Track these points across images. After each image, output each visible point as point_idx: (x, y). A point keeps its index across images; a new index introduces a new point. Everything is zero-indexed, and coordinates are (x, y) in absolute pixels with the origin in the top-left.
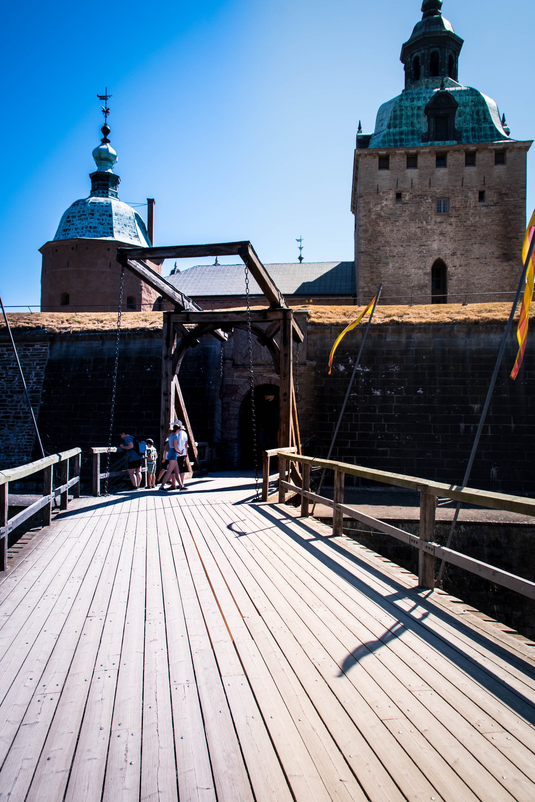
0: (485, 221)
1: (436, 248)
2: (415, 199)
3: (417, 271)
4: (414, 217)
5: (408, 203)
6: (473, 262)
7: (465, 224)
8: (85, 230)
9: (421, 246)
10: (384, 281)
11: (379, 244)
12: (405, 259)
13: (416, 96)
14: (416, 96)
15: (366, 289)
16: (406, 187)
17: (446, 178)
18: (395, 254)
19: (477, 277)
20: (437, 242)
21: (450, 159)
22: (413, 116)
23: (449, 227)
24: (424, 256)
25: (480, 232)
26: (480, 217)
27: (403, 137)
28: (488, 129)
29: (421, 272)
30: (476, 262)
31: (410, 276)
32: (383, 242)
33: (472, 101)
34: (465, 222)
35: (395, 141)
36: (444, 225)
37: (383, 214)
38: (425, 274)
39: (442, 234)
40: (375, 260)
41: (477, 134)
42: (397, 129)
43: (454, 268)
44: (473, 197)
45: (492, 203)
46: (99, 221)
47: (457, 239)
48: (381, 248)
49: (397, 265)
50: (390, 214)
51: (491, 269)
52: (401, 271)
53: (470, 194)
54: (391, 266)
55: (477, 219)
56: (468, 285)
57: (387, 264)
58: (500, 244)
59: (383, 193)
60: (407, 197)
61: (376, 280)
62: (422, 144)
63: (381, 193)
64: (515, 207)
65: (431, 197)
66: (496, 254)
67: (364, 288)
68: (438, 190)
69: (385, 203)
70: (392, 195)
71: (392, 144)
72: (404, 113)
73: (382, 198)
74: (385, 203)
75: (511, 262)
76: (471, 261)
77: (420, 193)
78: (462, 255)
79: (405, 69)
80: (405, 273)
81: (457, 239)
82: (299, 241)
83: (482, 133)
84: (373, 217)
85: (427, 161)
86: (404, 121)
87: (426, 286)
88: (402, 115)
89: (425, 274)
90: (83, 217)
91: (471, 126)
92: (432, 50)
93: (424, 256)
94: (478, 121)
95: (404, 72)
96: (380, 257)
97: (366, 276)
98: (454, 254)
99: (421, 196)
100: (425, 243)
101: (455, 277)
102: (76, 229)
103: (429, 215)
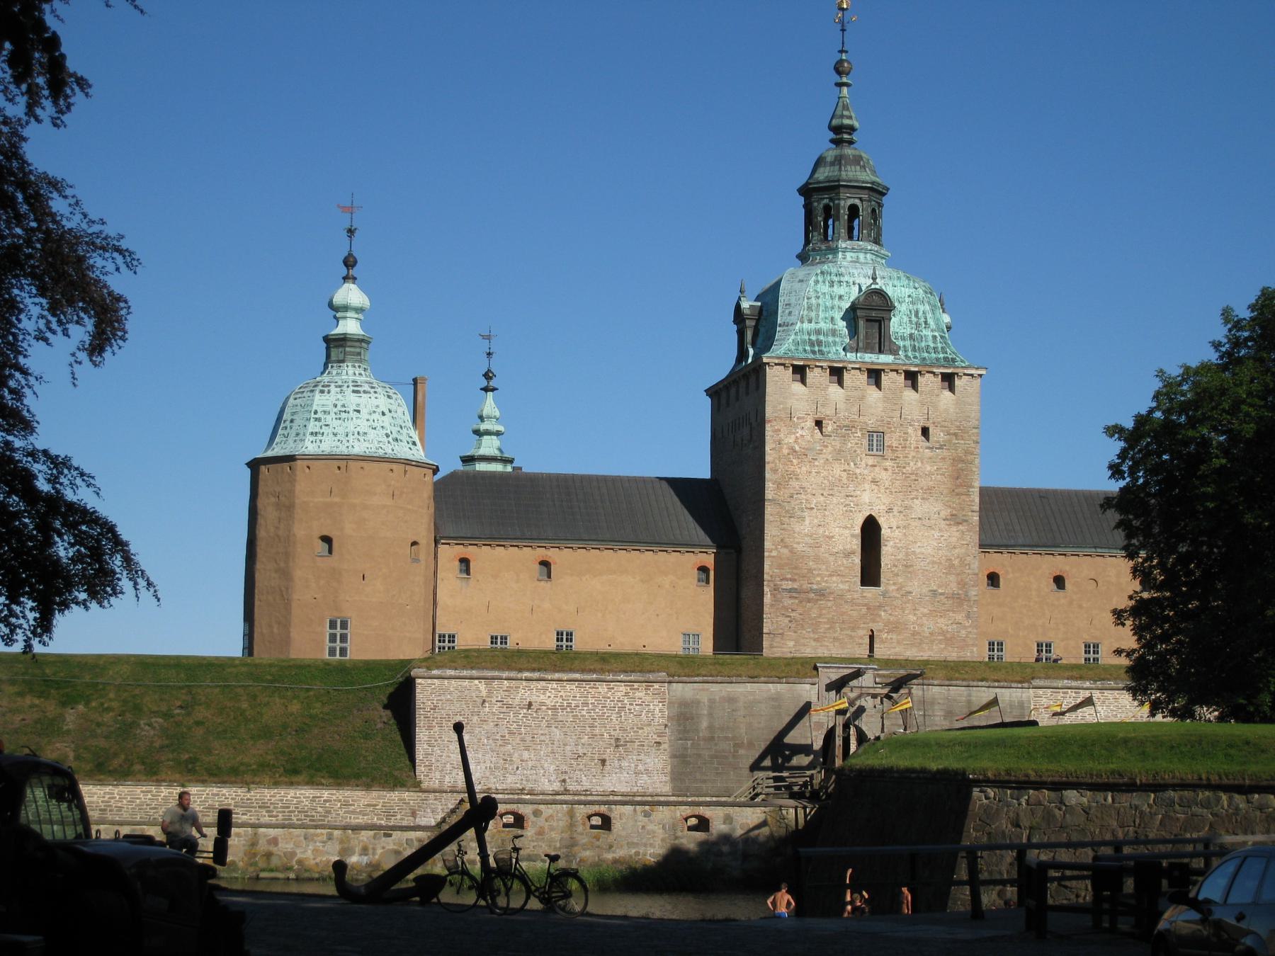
4: (839, 455)
6: (914, 524)
8: (351, 438)
13: (836, 279)
14: (836, 279)
15: (774, 553)
23: (884, 474)
27: (821, 337)
30: (917, 523)
35: (812, 344)
37: (797, 448)
38: (853, 536)
39: (874, 481)
40: (787, 511)
42: (813, 326)
44: (915, 435)
51: (937, 534)
52: (821, 531)
53: (910, 430)
54: (807, 522)
55: (919, 464)
56: (907, 555)
57: (803, 519)
60: (829, 427)
64: (967, 452)
66: (943, 514)
68: (871, 423)
69: (800, 432)
70: (810, 423)
71: (808, 348)
72: (820, 301)
73: (795, 426)
74: (800, 432)
75: (961, 527)
77: (846, 423)
79: (805, 206)
82: (488, 338)
83: (923, 344)
86: (822, 315)
88: (818, 305)
91: (908, 331)
92: (850, 202)
94: (918, 325)
98: (890, 510)
99: (848, 428)
102: (335, 435)
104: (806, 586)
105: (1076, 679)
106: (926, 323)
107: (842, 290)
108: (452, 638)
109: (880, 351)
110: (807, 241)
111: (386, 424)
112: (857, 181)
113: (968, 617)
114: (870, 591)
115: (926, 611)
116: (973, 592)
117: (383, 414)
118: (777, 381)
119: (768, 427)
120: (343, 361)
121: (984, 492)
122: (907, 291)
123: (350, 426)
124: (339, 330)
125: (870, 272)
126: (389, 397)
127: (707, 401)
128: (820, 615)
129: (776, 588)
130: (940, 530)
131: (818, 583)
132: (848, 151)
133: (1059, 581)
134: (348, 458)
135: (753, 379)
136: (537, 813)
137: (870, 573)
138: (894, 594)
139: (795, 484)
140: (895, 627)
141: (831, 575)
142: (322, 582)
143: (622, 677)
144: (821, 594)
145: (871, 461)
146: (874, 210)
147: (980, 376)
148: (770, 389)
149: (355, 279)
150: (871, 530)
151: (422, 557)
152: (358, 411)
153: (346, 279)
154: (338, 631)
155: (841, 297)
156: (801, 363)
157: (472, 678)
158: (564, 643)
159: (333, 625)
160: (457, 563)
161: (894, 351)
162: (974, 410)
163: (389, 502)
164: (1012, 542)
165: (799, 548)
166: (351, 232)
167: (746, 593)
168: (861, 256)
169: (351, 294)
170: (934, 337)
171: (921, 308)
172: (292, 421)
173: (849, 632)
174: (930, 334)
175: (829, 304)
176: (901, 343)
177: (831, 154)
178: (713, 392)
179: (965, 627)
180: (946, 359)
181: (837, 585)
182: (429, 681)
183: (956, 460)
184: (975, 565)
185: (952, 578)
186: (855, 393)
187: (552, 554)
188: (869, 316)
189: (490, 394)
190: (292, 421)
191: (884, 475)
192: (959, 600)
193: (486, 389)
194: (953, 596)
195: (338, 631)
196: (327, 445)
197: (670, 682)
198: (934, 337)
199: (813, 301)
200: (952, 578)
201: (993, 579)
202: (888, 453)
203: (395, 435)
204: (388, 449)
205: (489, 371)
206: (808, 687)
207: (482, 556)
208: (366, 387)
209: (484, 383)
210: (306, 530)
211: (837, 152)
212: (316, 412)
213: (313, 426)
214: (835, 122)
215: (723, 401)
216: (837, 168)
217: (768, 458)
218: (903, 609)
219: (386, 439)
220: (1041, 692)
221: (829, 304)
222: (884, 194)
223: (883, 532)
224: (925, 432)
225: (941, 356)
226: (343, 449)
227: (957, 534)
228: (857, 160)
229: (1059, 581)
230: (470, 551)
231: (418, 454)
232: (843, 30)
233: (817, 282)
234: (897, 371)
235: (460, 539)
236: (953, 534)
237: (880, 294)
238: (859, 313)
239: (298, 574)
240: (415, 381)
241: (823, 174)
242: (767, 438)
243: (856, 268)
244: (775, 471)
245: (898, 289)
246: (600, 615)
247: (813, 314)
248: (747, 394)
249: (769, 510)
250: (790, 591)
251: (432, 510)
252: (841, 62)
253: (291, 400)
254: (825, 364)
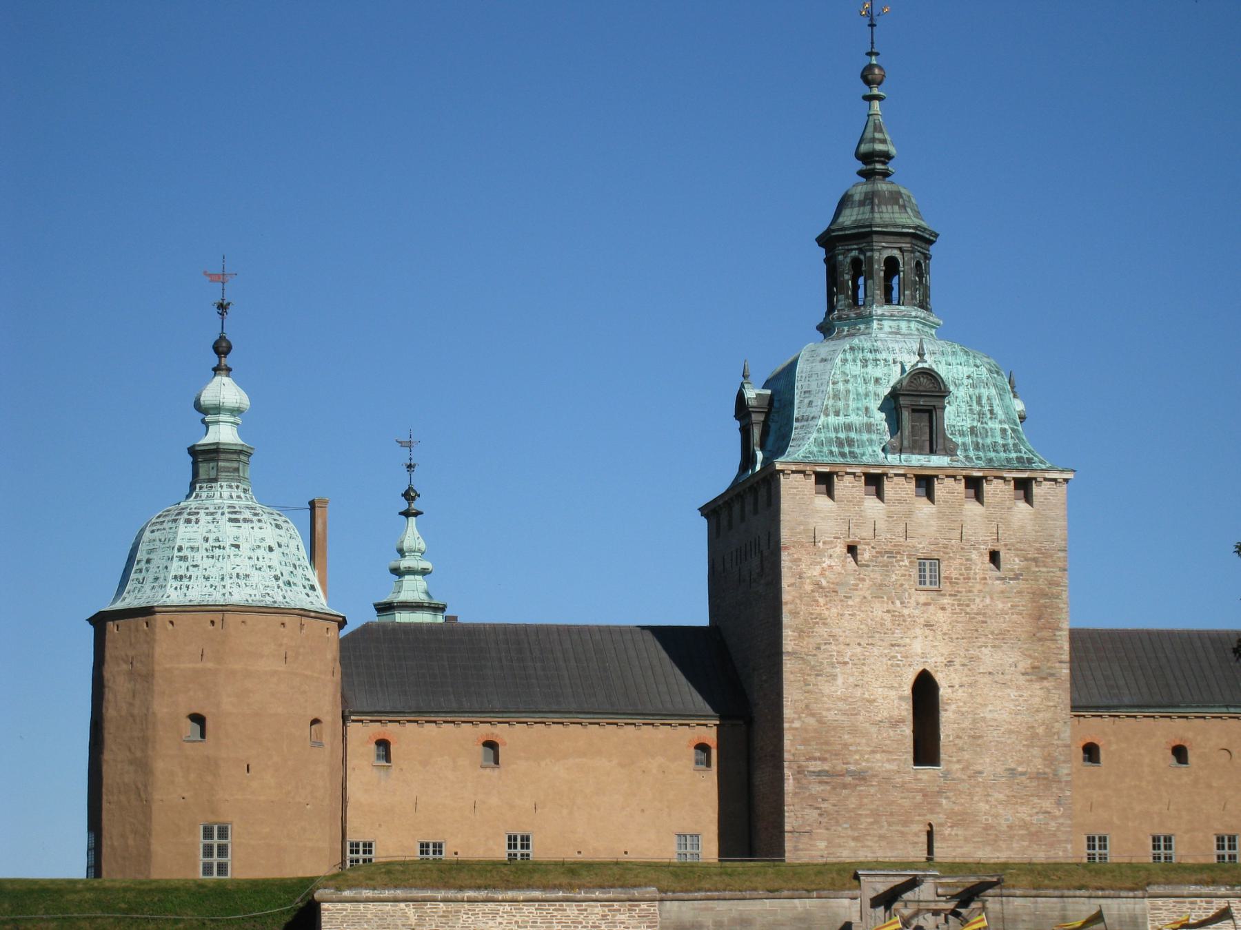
0: (1000, 606)
1: (920, 651)
2: (880, 559)
3: (886, 692)
4: (880, 590)
5: (868, 566)
7: (968, 610)
8: (228, 582)
9: (892, 645)
10: (829, 710)
11: (819, 640)
12: (866, 669)
13: (869, 356)
14: (869, 356)
15: (797, 724)
16: (864, 535)
17: (932, 522)
18: (847, 660)
19: (990, 708)
20: (920, 639)
21: (939, 489)
22: (867, 395)
23: (940, 614)
24: (898, 666)
25: (994, 625)
26: (992, 598)
27: (853, 435)
28: (998, 433)
29: (893, 693)
30: (987, 679)
31: (874, 701)
32: (826, 636)
33: (969, 377)
34: (968, 605)
35: (840, 443)
36: (932, 608)
37: (824, 583)
38: (901, 698)
39: (928, 625)
40: (813, 668)
41: (980, 440)
42: (841, 419)
43: (950, 690)
44: (981, 561)
45: (1011, 575)
46: (252, 562)
47: (954, 636)
48: (823, 647)
49: (851, 680)
50: (837, 584)
52: (858, 692)
54: (840, 681)
55: (988, 601)
56: (974, 721)
57: (834, 677)
58: (1027, 649)
59: (824, 543)
60: (865, 554)
61: (813, 706)
62: (893, 459)
63: (820, 544)
64: (1051, 583)
65: (909, 556)
67: (792, 722)
68: (922, 546)
69: (828, 562)
70: (841, 549)
71: (835, 449)
72: (850, 386)
73: (821, 553)
74: (828, 562)
75: (1045, 683)
76: (978, 678)
77: (887, 548)
78: (964, 665)
79: (827, 261)
80: (866, 696)
81: (954, 636)
83: (989, 441)
84: (808, 588)
86: (852, 405)
87: (903, 722)
88: (848, 391)
89: (901, 698)
90: (217, 552)
91: (968, 424)
93: (898, 666)
95: (824, 266)
96: (822, 663)
97: (795, 698)
98: (950, 663)
100: (900, 641)
101: (953, 707)
102: (207, 578)
103: (905, 590)
104: (840, 767)
105: (1207, 884)
106: (991, 412)
107: (878, 372)
108: (368, 847)
109: (932, 451)
110: (831, 307)
111: (275, 563)
112: (895, 226)
113: (1059, 803)
114: (926, 772)
115: (1001, 797)
116: (1064, 770)
117: (271, 549)
118: (796, 493)
119: (785, 557)
120: (215, 480)
121: (1077, 637)
122: (966, 371)
123: (227, 566)
124: (209, 439)
125: (916, 347)
126: (278, 526)
127: (701, 526)
128: (861, 806)
129: (800, 771)
130: (1018, 688)
131: (857, 762)
132: (882, 186)
133: (1180, 753)
134: (224, 609)
135: (763, 492)
137: (926, 748)
138: (959, 775)
139: (821, 630)
140: (962, 819)
141: (873, 752)
142: (192, 776)
143: (597, 894)
144: (861, 777)
145: (923, 597)
146: (918, 264)
147: (1066, 480)
148: (785, 505)
149: (229, 370)
151: (326, 739)
152: (237, 547)
153: (217, 370)
154: (216, 841)
155: (877, 380)
156: (827, 469)
157: (396, 900)
158: (519, 851)
159: (208, 833)
160: (373, 746)
161: (950, 451)
162: (1059, 528)
163: (281, 667)
164: (1115, 702)
165: (830, 716)
166: (223, 307)
167: (761, 777)
168: (903, 325)
169: (225, 391)
170: (1003, 431)
171: (985, 392)
172: (148, 561)
173: (899, 828)
174: (997, 426)
175: (861, 390)
176: (959, 440)
177: (861, 189)
178: (711, 511)
179: (1054, 818)
180: (1019, 459)
181: (881, 764)
182: (339, 906)
183: (1038, 594)
184: (1066, 734)
185: (1036, 751)
186: (899, 508)
187: (499, 732)
188: (916, 405)
189: (412, 520)
190: (148, 561)
191: (941, 616)
192: (1046, 780)
193: (407, 514)
194: (1039, 776)
195: (216, 841)
196: (196, 593)
197: (661, 900)
198: (1003, 431)
199: (841, 386)
200: (1036, 751)
201: (1091, 752)
202: (946, 587)
203: (286, 577)
204: (278, 597)
205: (410, 489)
206: (846, 902)
207: (404, 735)
208: (247, 514)
209: (404, 505)
210: (169, 708)
212: (180, 549)
213: (176, 568)
214: (864, 148)
215: (724, 522)
216: (868, 208)
217: (785, 597)
218: (971, 795)
219: (274, 583)
220: (1160, 902)
221: (861, 390)
222: (931, 242)
223: (942, 692)
224: (994, 557)
225: (1014, 455)
226: (217, 598)
227: (1040, 693)
228: (895, 198)
229: (1180, 753)
230: (391, 730)
231: (319, 601)
232: (872, 25)
233: (845, 361)
234: (954, 477)
235: (377, 714)
236: (1036, 692)
237: (930, 374)
238: (902, 401)
239: (160, 765)
240: (312, 505)
241: (849, 217)
242: (785, 571)
243: (894, 343)
244: (795, 614)
245: (954, 368)
246: (565, 812)
247: (841, 404)
248: (756, 512)
249: (788, 665)
250: (819, 773)
251: (338, 676)
252: (870, 67)
253: (147, 534)
254: (858, 470)
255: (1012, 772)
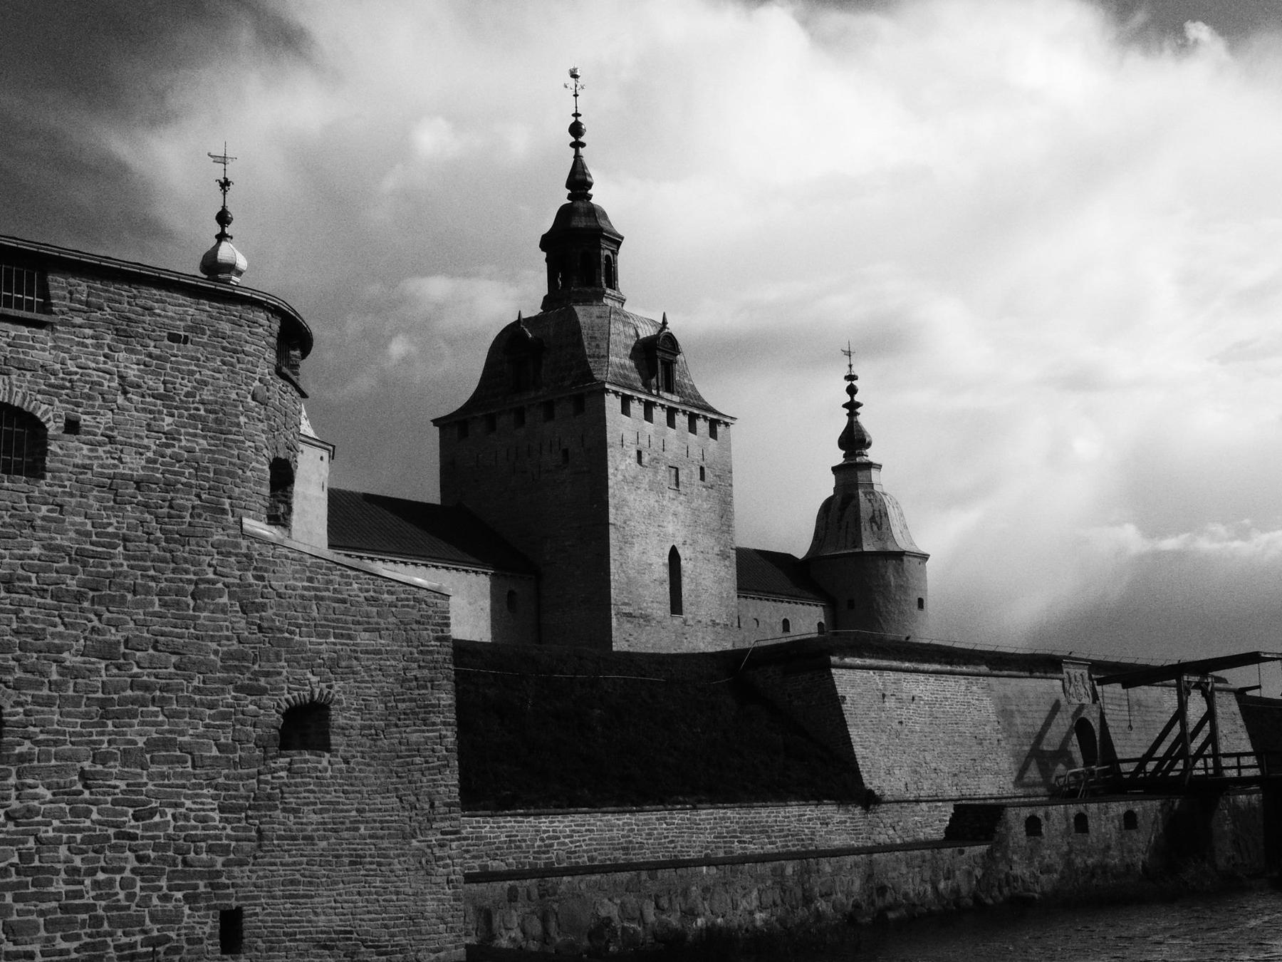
30: (700, 556)
39: (675, 515)
60: (645, 459)
70: (634, 453)
85: (659, 415)
114: (677, 621)
136: (1047, 816)
137: (676, 606)
144: (647, 618)
150: (674, 556)
166: (225, 184)
211: (579, 204)
224: (702, 469)
255: (714, 624)
